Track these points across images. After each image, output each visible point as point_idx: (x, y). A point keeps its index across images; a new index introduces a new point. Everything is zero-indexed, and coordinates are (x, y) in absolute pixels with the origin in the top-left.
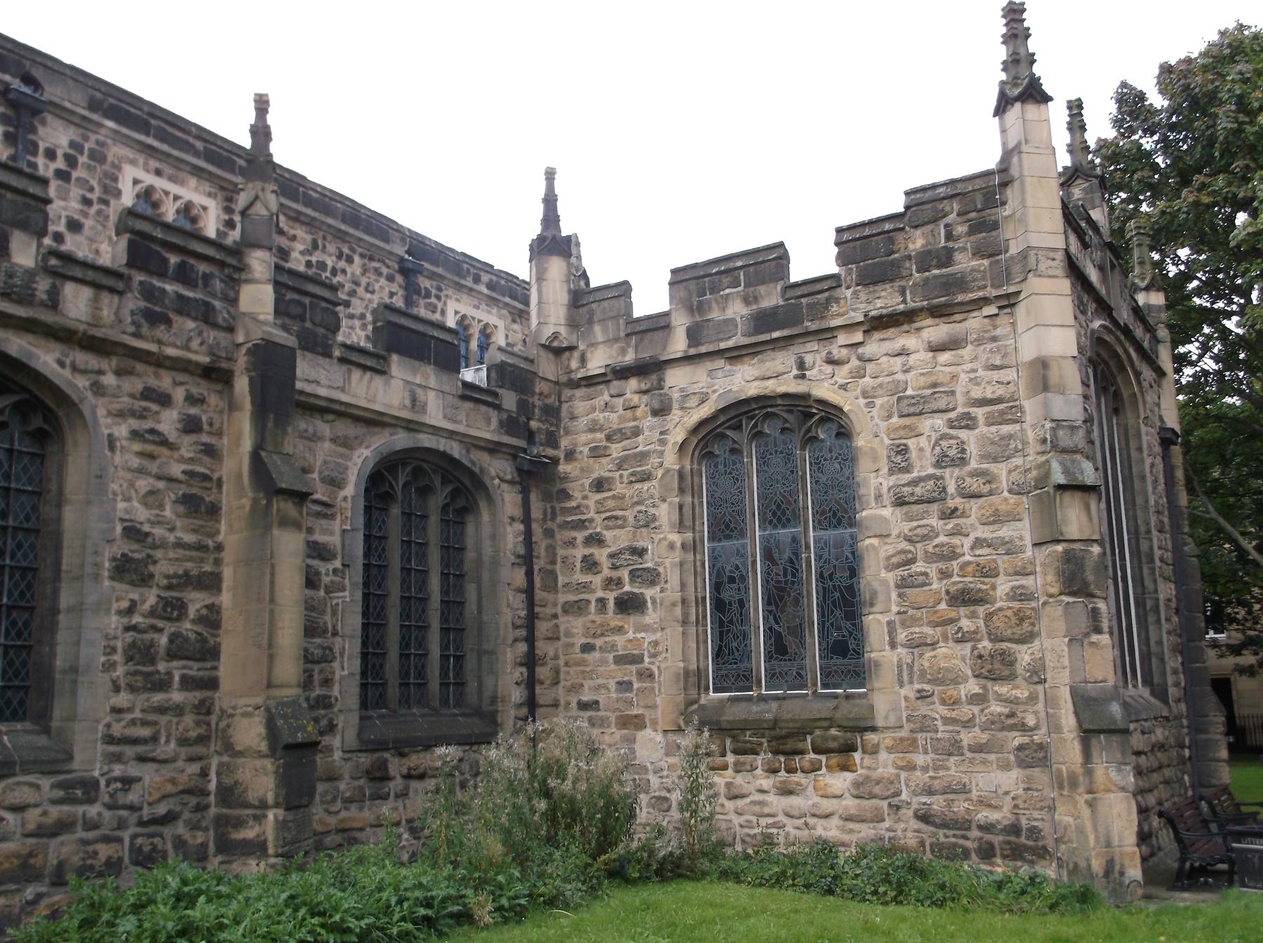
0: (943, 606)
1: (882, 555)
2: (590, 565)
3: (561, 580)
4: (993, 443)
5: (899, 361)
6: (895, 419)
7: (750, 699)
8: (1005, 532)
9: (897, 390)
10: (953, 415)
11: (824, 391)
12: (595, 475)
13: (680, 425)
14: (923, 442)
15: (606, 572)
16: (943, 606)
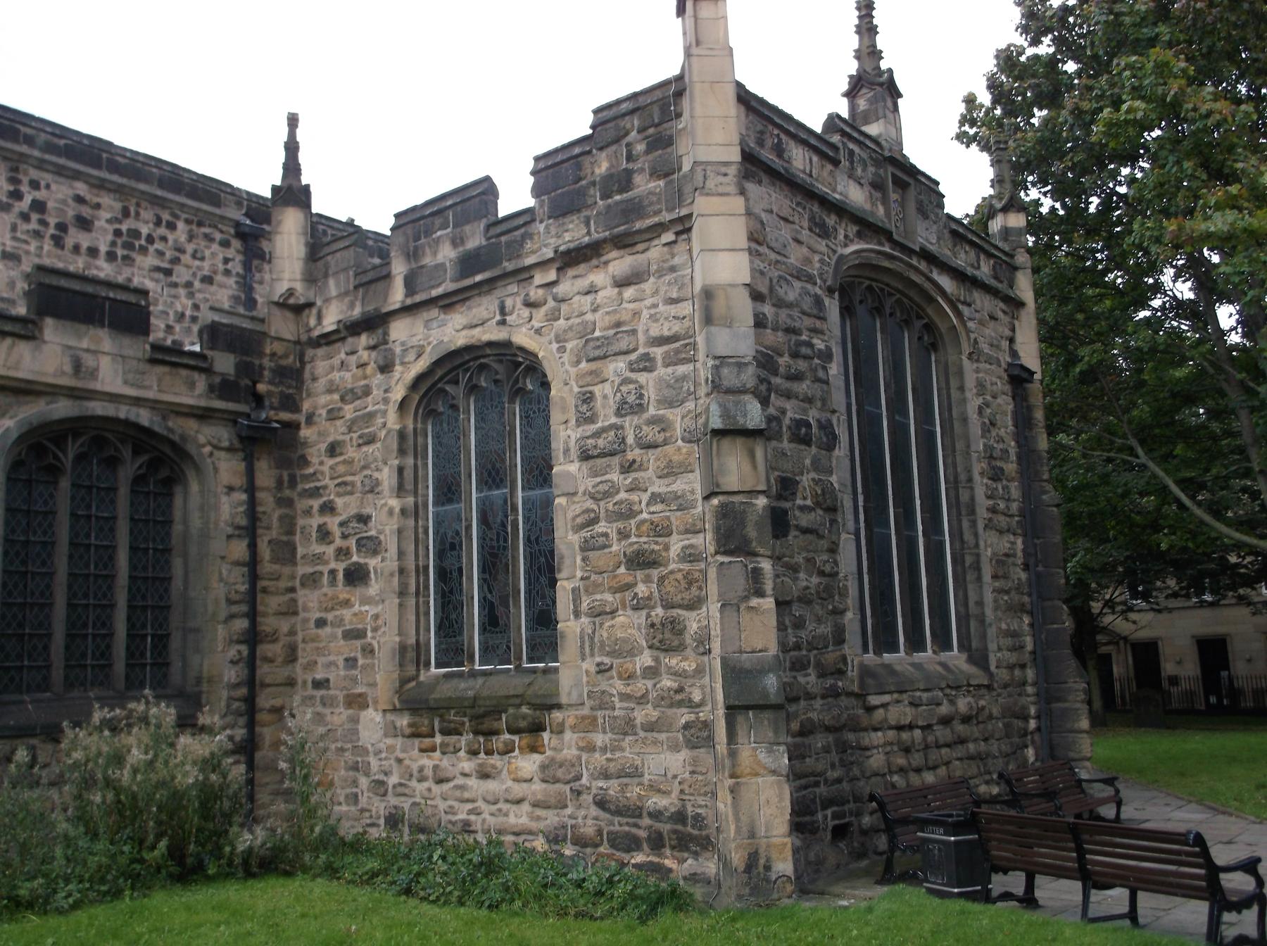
0: (622, 570)
1: (570, 515)
2: (324, 535)
3: (300, 551)
4: (669, 386)
5: (589, 298)
6: (583, 365)
7: (460, 675)
8: (679, 485)
9: (585, 332)
10: (633, 357)
11: (522, 338)
12: (330, 439)
14: (607, 389)
15: (339, 542)
16: (622, 570)
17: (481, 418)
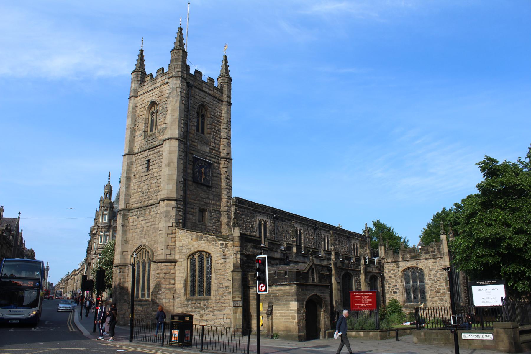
2: (389, 287)
13: (401, 269)
17: (412, 274)
